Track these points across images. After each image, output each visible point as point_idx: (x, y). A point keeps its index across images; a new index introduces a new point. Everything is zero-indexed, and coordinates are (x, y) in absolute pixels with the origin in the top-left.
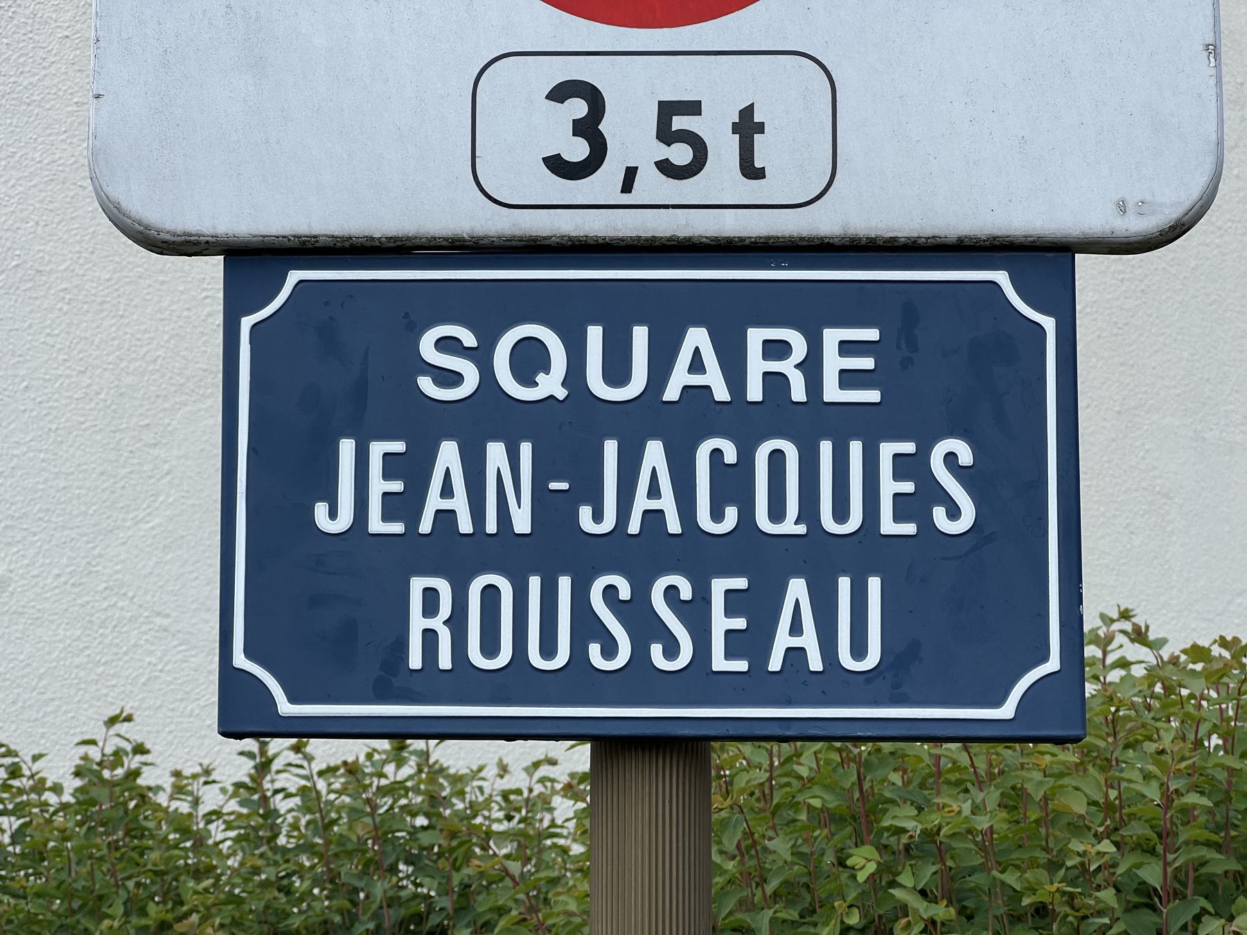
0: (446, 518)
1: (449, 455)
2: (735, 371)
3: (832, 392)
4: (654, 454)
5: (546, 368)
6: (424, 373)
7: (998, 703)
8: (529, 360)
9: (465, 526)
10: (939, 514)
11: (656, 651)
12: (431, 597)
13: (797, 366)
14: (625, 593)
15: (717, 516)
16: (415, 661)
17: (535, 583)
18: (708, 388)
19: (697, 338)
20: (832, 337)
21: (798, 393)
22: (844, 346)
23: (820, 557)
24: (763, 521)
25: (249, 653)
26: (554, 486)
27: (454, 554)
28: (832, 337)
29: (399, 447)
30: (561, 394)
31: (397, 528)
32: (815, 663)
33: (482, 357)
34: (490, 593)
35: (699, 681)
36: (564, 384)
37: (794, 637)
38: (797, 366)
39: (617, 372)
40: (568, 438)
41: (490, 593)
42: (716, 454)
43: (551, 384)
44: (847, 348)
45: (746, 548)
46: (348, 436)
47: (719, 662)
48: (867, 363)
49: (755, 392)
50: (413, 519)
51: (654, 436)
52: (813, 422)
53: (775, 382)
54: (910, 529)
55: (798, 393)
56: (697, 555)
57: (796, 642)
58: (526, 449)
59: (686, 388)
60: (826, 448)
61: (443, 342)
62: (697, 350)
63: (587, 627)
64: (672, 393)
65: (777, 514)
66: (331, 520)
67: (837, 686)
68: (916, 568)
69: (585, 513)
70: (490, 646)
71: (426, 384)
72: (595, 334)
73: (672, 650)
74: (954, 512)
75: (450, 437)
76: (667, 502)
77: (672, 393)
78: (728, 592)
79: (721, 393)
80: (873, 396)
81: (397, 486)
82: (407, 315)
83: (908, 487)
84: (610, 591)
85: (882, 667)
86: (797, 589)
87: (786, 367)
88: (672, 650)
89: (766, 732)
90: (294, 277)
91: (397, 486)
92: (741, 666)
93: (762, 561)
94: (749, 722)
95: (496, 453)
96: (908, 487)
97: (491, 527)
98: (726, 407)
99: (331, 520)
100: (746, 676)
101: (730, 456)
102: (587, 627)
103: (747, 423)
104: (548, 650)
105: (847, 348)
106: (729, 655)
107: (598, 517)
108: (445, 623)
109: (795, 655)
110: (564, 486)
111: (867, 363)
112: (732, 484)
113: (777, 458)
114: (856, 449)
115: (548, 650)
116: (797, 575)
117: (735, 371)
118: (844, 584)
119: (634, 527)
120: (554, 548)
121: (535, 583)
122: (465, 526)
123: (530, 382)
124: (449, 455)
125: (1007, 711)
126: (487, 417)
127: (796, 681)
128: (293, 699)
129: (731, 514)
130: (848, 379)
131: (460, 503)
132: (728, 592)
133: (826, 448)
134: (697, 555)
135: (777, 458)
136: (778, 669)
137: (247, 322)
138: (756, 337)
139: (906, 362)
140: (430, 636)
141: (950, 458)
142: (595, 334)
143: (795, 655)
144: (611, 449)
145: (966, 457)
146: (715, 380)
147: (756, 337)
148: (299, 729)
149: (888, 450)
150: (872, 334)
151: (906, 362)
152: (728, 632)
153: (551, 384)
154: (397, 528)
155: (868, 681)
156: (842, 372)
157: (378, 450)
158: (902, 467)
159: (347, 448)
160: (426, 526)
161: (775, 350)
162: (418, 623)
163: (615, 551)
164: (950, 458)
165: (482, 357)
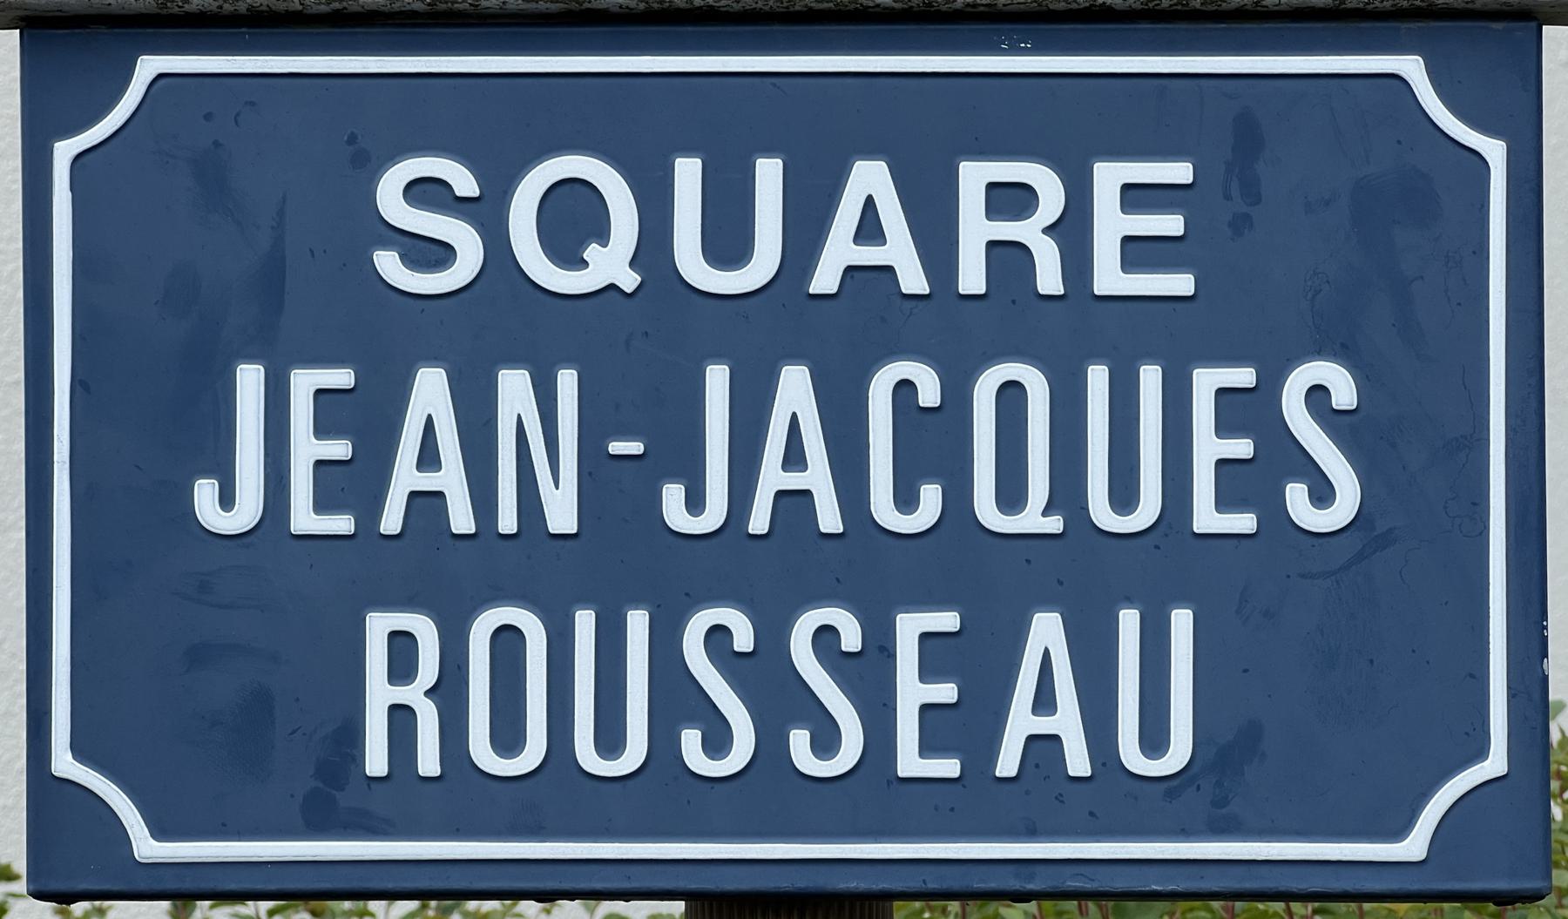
0: (427, 504)
1: (431, 393)
2: (937, 244)
3: (1110, 278)
4: (795, 390)
5: (603, 236)
6: (385, 245)
7: (1398, 832)
8: (572, 221)
9: (462, 519)
10: (1296, 497)
11: (799, 742)
12: (402, 648)
13: (1048, 230)
14: (744, 639)
15: (906, 500)
16: (376, 762)
17: (585, 623)
18: (889, 269)
19: (870, 179)
20: (1109, 177)
21: (1049, 278)
22: (1131, 193)
23: (1086, 575)
24: (987, 512)
25: (80, 751)
26: (617, 447)
27: (444, 570)
28: (1109, 177)
29: (341, 378)
30: (629, 281)
31: (342, 524)
32: (1078, 762)
33: (487, 213)
34: (507, 641)
35: (874, 795)
36: (633, 263)
37: (1041, 714)
38: (1048, 230)
39: (727, 239)
40: (640, 357)
41: (507, 641)
42: (905, 388)
43: (611, 264)
44: (1135, 197)
45: (959, 562)
46: (251, 358)
47: (910, 762)
48: (1171, 224)
49: (972, 277)
50: (370, 509)
51: (795, 358)
52: (1077, 330)
53: (1008, 259)
54: (1244, 522)
55: (1049, 278)
56: (872, 571)
57: (1044, 725)
58: (567, 382)
59: (850, 270)
60: (1098, 378)
61: (416, 189)
62: (870, 203)
63: (677, 699)
64: (825, 279)
65: (1011, 495)
66: (224, 511)
67: (1114, 799)
68: (1251, 591)
69: (673, 496)
70: (508, 737)
71: (388, 264)
72: (688, 174)
73: (826, 742)
74: (1322, 494)
75: (433, 360)
76: (818, 478)
77: (825, 279)
78: (925, 637)
79: (913, 280)
80: (1181, 284)
81: (340, 449)
82: (352, 140)
83: (1242, 448)
84: (718, 636)
85: (1195, 769)
86: (1047, 632)
87: (1029, 231)
88: (826, 742)
89: (992, 885)
90: (148, 67)
91: (340, 449)
92: (948, 767)
93: (986, 583)
94: (964, 868)
95: (514, 390)
96: (1242, 448)
97: (508, 522)
98: (921, 304)
99: (224, 511)
100: (958, 786)
101: (929, 393)
102: (677, 699)
103: (960, 331)
104: (610, 739)
105: (1135, 197)
106: (928, 748)
107: (695, 503)
108: (428, 693)
109: (1043, 747)
110: (635, 448)
111: (1171, 224)
112: (932, 443)
113: (1011, 393)
114: (1150, 378)
115: (610, 739)
116: (1047, 604)
117: (937, 244)
118: (1129, 622)
119: (759, 522)
120: (619, 559)
121: (585, 623)
122: (462, 519)
123: (572, 260)
124: (431, 393)
125: (1414, 846)
126: (498, 323)
127: (1043, 793)
128: (160, 832)
129: (931, 498)
130: (1137, 253)
131: (451, 479)
132: (925, 637)
133: (1098, 378)
134: (872, 571)
135: (1011, 393)
136: (1013, 773)
137: (64, 151)
138: (974, 177)
139: (1240, 224)
140: (401, 716)
141: (1317, 395)
142: (688, 174)
143: (1043, 747)
144: (717, 379)
145: (1344, 393)
146: (900, 253)
147: (974, 177)
148: (172, 885)
149: (1207, 382)
150: (1179, 172)
151: (1240, 224)
152: (926, 709)
153: (611, 264)
154: (342, 524)
155: (1171, 795)
156: (1127, 240)
157: (305, 383)
158: (1235, 411)
159: (250, 380)
160: (392, 520)
161: (1010, 200)
162: (379, 694)
163: (725, 563)
164: (1317, 395)
165: (487, 213)
